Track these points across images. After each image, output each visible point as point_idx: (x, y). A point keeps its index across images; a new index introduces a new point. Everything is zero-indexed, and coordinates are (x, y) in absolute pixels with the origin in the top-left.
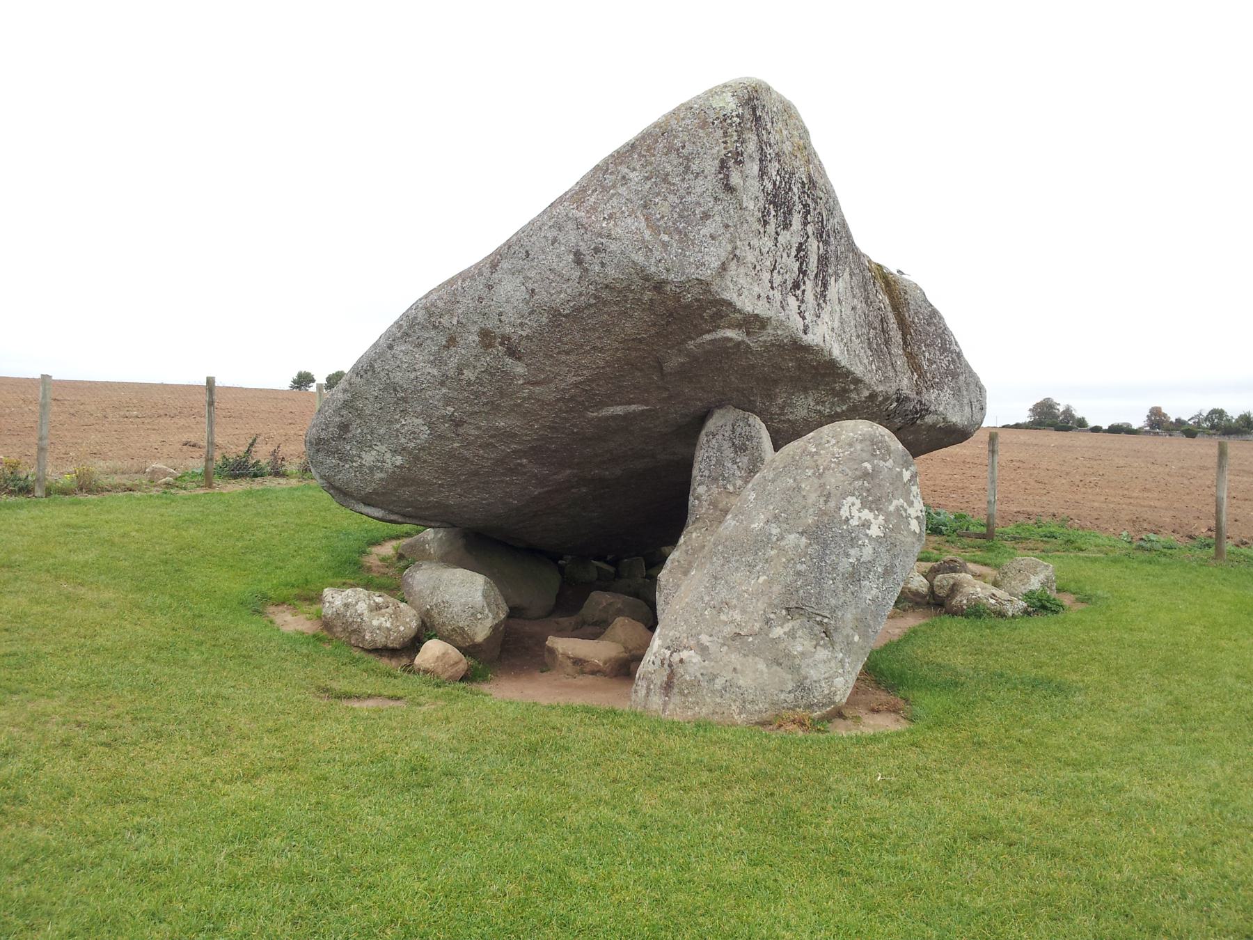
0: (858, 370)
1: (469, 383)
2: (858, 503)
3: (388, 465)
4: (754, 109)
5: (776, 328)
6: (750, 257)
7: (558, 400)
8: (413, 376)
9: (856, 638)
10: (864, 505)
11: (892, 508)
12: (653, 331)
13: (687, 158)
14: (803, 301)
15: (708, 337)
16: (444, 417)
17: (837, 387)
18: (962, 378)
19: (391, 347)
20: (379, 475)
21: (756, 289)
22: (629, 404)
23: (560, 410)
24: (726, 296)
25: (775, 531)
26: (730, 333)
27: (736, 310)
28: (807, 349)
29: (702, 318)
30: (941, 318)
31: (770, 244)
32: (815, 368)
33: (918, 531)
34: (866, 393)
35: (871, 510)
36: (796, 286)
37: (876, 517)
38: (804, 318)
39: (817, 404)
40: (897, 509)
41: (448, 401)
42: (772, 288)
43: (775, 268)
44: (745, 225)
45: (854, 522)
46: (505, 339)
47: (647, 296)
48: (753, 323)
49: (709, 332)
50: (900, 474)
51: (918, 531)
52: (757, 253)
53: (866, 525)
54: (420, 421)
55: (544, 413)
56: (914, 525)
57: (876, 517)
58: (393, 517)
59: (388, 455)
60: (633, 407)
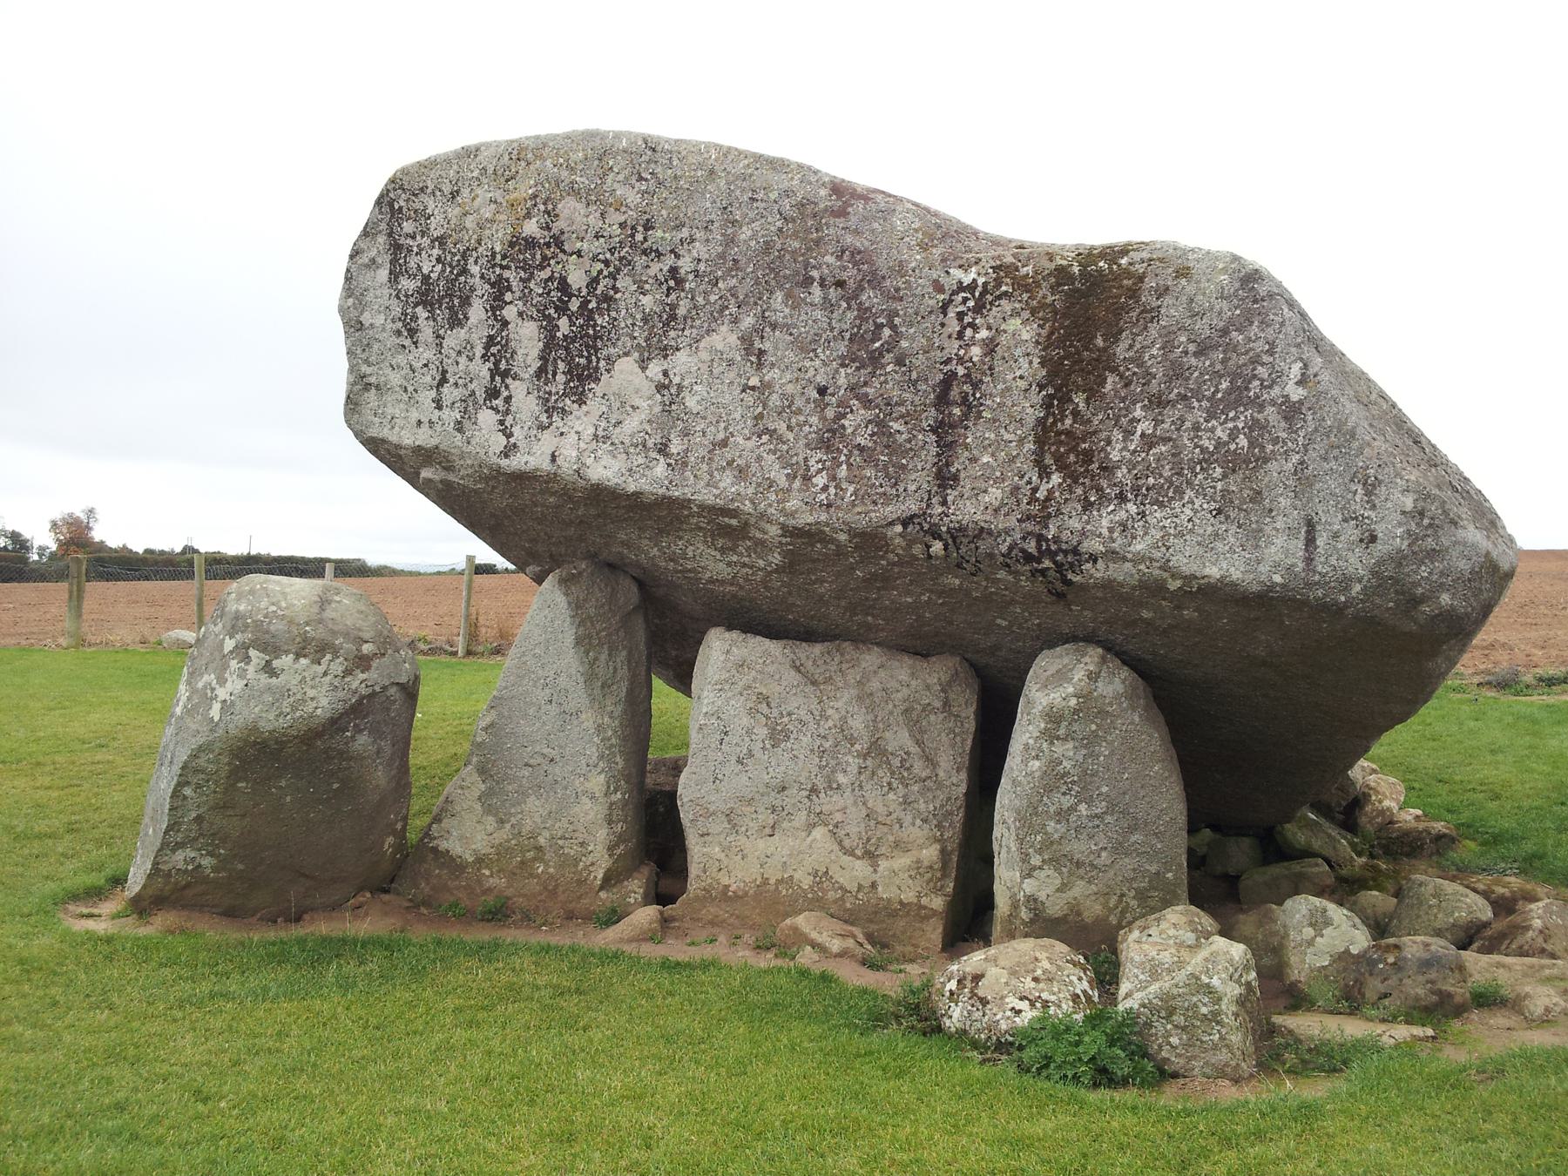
6: (395, 379)
18: (1277, 470)
21: (414, 415)
28: (522, 478)
33: (216, 719)
36: (493, 393)
38: (509, 436)
42: (439, 408)
44: (376, 346)
51: (216, 719)
52: (407, 371)
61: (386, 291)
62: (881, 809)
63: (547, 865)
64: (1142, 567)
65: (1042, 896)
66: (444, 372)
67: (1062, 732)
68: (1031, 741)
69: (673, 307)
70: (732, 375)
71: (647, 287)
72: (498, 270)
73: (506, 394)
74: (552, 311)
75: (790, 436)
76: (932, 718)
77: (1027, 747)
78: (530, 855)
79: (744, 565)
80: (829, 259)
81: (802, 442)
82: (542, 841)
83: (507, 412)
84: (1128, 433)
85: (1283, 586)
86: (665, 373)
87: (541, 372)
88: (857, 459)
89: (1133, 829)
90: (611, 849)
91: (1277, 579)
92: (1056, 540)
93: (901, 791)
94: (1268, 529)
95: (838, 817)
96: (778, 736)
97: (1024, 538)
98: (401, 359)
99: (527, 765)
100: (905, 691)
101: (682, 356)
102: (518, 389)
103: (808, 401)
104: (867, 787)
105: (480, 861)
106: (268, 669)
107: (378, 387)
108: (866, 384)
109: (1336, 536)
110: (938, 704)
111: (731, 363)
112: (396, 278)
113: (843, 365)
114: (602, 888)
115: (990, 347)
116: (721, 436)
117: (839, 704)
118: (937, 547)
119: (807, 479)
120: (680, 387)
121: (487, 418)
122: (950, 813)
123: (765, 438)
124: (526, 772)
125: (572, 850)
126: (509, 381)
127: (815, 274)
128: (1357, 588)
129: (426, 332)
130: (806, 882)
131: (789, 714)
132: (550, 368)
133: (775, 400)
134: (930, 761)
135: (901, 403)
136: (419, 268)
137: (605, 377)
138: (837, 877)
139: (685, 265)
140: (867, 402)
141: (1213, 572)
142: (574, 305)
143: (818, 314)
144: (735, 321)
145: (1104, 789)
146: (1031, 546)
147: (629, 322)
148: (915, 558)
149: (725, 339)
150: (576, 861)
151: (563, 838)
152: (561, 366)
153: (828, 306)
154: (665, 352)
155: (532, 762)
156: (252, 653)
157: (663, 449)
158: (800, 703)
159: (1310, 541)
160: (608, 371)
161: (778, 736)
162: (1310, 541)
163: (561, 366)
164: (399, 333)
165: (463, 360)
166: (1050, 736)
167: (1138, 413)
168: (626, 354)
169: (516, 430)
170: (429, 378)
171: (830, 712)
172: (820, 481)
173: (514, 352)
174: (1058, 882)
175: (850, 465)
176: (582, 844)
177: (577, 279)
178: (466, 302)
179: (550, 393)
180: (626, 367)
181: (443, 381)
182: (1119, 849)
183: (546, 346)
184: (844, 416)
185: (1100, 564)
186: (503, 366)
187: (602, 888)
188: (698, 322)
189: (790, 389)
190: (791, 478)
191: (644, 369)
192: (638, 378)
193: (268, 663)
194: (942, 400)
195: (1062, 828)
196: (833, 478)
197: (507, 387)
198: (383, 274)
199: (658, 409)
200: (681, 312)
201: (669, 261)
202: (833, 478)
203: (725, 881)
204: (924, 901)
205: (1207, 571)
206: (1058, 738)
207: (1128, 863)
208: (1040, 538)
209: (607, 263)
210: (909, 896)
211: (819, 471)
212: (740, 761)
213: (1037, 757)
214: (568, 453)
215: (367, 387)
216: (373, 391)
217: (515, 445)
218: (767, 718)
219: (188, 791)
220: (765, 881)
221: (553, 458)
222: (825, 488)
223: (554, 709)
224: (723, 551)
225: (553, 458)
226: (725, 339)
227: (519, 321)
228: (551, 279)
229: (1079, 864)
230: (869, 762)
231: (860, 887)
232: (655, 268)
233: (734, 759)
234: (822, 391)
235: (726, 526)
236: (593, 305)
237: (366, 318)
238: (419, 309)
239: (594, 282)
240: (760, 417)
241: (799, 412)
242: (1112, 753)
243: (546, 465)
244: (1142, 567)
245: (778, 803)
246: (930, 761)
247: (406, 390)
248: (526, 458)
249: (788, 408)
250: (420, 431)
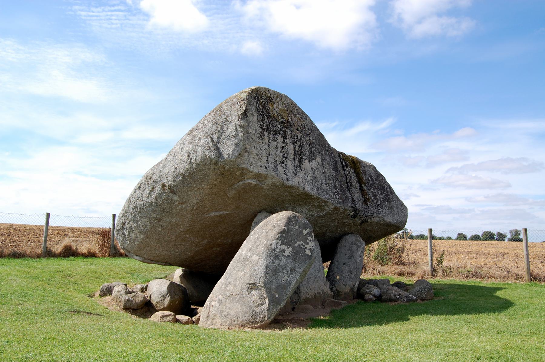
0: (324, 197)
1: (160, 205)
2: (280, 243)
3: (139, 239)
5: (272, 179)
6: (255, 151)
7: (192, 210)
8: (142, 203)
9: (277, 296)
10: (282, 244)
11: (296, 245)
12: (219, 180)
13: (227, 116)
14: (286, 168)
15: (241, 183)
16: (153, 218)
17: (316, 204)
19: (135, 192)
20: (137, 243)
21: (259, 164)
22: (220, 211)
23: (194, 214)
24: (244, 166)
25: (249, 254)
26: (250, 181)
27: (249, 172)
28: (290, 187)
29: (236, 175)
30: (383, 178)
31: (266, 146)
32: (299, 195)
33: (310, 254)
34: (332, 207)
35: (286, 245)
37: (288, 248)
38: (287, 175)
39: (309, 211)
40: (299, 245)
41: (154, 212)
43: (269, 155)
44: (251, 140)
45: (278, 250)
46: (170, 186)
47: (213, 167)
48: (258, 177)
49: (241, 181)
50: (302, 231)
51: (310, 254)
53: (283, 251)
54: (146, 220)
55: (189, 215)
56: (308, 252)
57: (288, 248)
58: (146, 261)
59: (138, 234)
60: (222, 212)
87: (294, 159)
101: (314, 161)
102: (289, 163)
129: (266, 140)
141: (389, 220)
149: (319, 159)
154: (312, 160)
186: (286, 155)
224: (309, 211)
243: (297, 185)
250: (262, 169)
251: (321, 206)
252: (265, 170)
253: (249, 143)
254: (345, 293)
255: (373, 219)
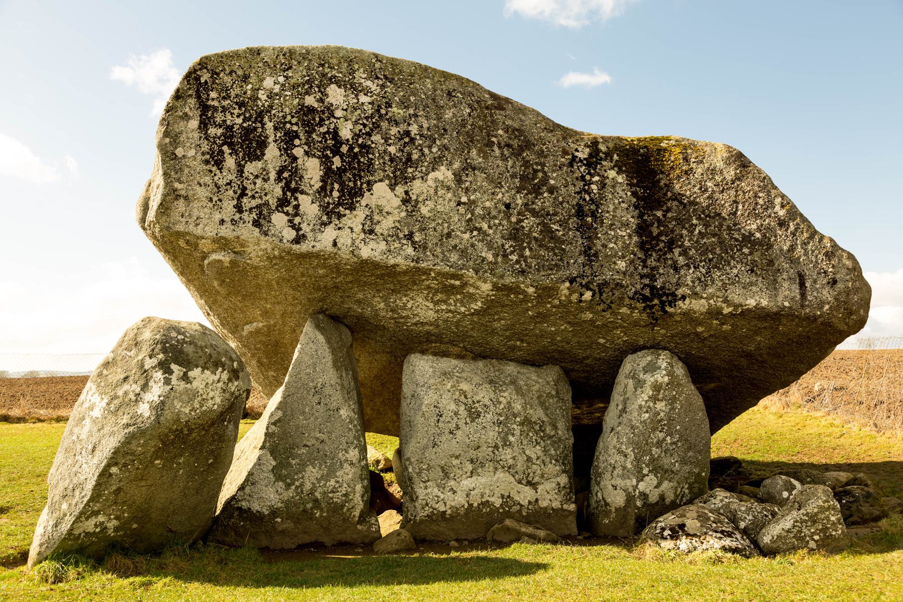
4: (198, 79)
21: (217, 217)
26: (214, 257)
34: (486, 287)
36: (283, 203)
38: (297, 228)
39: (436, 303)
44: (186, 171)
52: (212, 186)
60: (255, 324)
61: (196, 135)
62: (534, 456)
63: (322, 510)
64: (712, 301)
65: (648, 491)
66: (244, 189)
67: (660, 396)
68: (643, 403)
69: (410, 155)
70: (450, 195)
71: (390, 141)
72: (288, 126)
73: (296, 203)
74: (328, 152)
75: (491, 232)
76: (551, 400)
77: (640, 407)
78: (309, 506)
79: (450, 311)
80: (500, 132)
81: (499, 235)
82: (318, 495)
83: (296, 215)
84: (692, 232)
85: (790, 308)
86: (407, 193)
87: (323, 188)
88: (534, 245)
89: (689, 449)
90: (362, 497)
91: (786, 304)
92: (662, 288)
93: (542, 444)
94: (779, 279)
95: (511, 462)
96: (474, 415)
97: (642, 289)
98: (207, 179)
99: (305, 446)
100: (537, 386)
101: (417, 183)
103: (500, 212)
104: (525, 442)
105: (274, 513)
106: (185, 378)
107: (186, 198)
108: (533, 203)
109: (815, 282)
110: (554, 393)
111: (449, 188)
112: (206, 125)
113: (518, 192)
114: (358, 523)
115: (603, 186)
116: (446, 231)
117: (506, 394)
118: (588, 295)
119: (505, 256)
120: (417, 201)
121: (279, 219)
122: (567, 455)
123: (475, 233)
124: (304, 451)
125: (337, 498)
126: (298, 195)
127: (494, 139)
128: (827, 307)
129: (230, 162)
130: (498, 502)
131: (478, 402)
132: (328, 188)
133: (479, 211)
134: (555, 427)
135: (555, 214)
136: (224, 121)
137: (367, 194)
138: (517, 498)
139: (414, 129)
140: (535, 213)
141: (751, 303)
142: (344, 149)
143: (500, 163)
144: (451, 164)
145: (678, 427)
146: (647, 292)
147: (381, 161)
148: (571, 302)
150: (343, 506)
151: (332, 492)
152: (336, 186)
153: (504, 158)
154: (406, 180)
155: (309, 444)
156: (174, 367)
157: (410, 237)
158: (484, 395)
159: (802, 285)
160: (369, 190)
161: (474, 415)
162: (802, 285)
163: (336, 186)
164: (207, 162)
165: (259, 181)
166: (654, 399)
167: (695, 222)
168: (381, 181)
169: (304, 226)
170: (231, 193)
171: (501, 399)
172: (514, 257)
173: (301, 177)
174: (655, 482)
175: (531, 249)
176: (346, 495)
177: (346, 132)
178: (263, 145)
179: (328, 203)
180: (381, 189)
181: (243, 194)
182: (683, 462)
183: (326, 174)
184: (522, 221)
185: (687, 301)
186: (293, 185)
187: (358, 523)
188: (426, 164)
189: (488, 204)
190: (496, 256)
191: (393, 190)
192: (389, 194)
193: (185, 374)
194: (580, 212)
195: (659, 451)
196: (521, 256)
197: (296, 199)
198: (194, 124)
199: (403, 214)
200: (415, 157)
201: (403, 127)
202: (521, 256)
203: (442, 509)
204: (565, 507)
205: (748, 302)
206: (658, 400)
207: (687, 468)
208: (652, 288)
209: (365, 125)
210: (556, 504)
211: (512, 253)
212: (451, 433)
213: (647, 412)
214: (345, 239)
215: (178, 197)
216: (182, 200)
217: (304, 236)
218: (466, 405)
219: (114, 470)
220: (471, 505)
221: (335, 244)
222: (518, 262)
223: (321, 408)
224: (436, 303)
225: (335, 244)
226: (444, 174)
227: (306, 158)
228: (328, 132)
229: (666, 471)
230: (525, 428)
231: (530, 502)
232: (394, 131)
233: (447, 431)
234: (508, 206)
235: (449, 287)
236: (356, 150)
237: (179, 152)
238: (225, 148)
239: (357, 136)
240: (470, 220)
241: (495, 217)
242: (682, 407)
243: (330, 249)
244: (712, 301)
245: (474, 457)
246: (555, 427)
247: (211, 200)
248: (313, 243)
249: (488, 215)
250: (223, 227)
251: (453, 286)
252: (232, 227)
253: (184, 179)
254: (616, 509)
255: (684, 305)
